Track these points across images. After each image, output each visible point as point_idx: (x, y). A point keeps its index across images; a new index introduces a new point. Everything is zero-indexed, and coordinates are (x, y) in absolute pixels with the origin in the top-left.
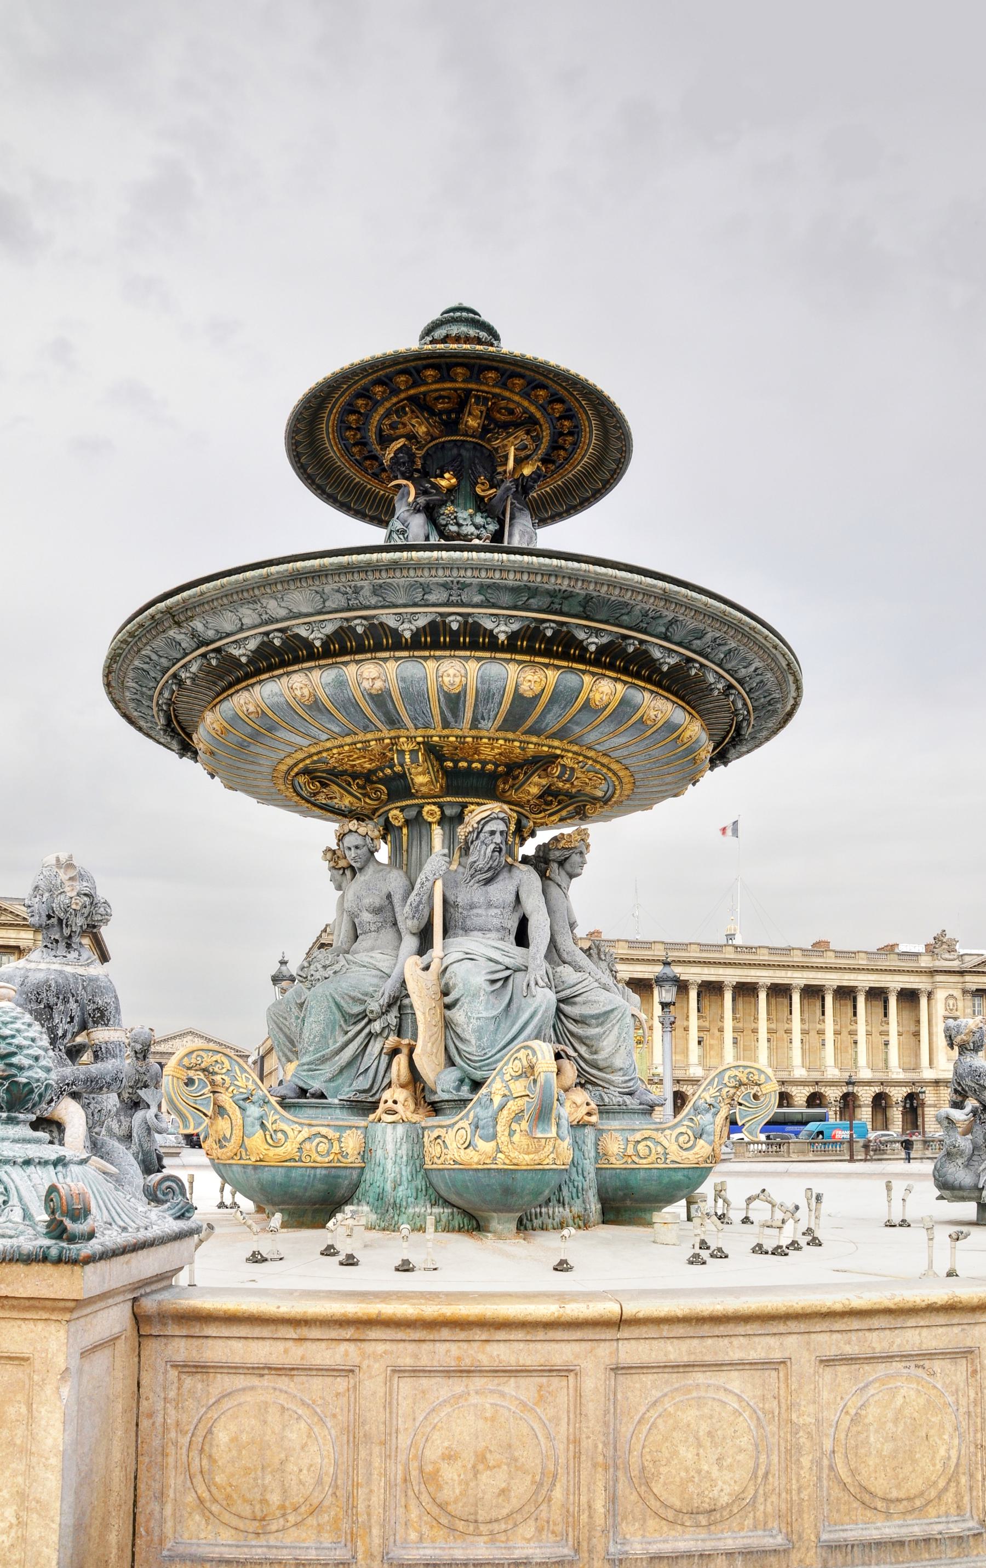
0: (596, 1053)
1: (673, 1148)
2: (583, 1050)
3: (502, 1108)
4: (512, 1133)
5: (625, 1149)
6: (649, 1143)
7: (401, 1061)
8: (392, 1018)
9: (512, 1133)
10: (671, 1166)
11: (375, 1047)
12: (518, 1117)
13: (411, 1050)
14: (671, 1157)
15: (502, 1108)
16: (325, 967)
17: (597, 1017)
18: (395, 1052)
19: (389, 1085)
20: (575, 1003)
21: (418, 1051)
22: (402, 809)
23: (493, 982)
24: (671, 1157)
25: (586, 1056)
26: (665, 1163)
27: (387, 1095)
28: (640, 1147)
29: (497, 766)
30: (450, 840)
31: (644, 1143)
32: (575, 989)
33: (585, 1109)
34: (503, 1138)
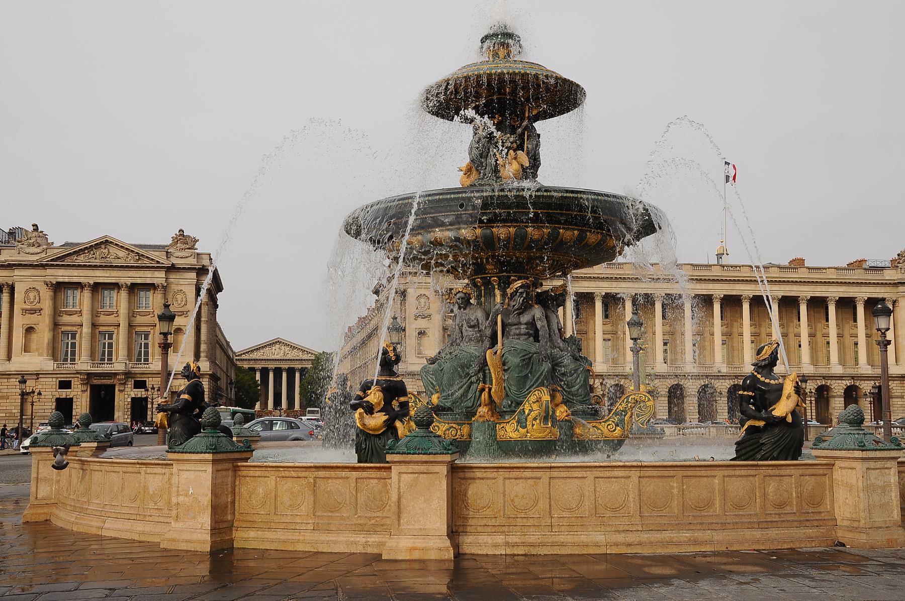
1: (605, 431)
3: (529, 415)
4: (533, 425)
7: (485, 396)
8: (481, 375)
9: (533, 425)
11: (474, 387)
12: (535, 419)
13: (490, 389)
15: (529, 415)
16: (450, 353)
18: (483, 390)
19: (480, 405)
21: (493, 390)
22: (481, 278)
23: (524, 360)
27: (480, 409)
30: (504, 295)
33: (565, 414)
34: (529, 427)
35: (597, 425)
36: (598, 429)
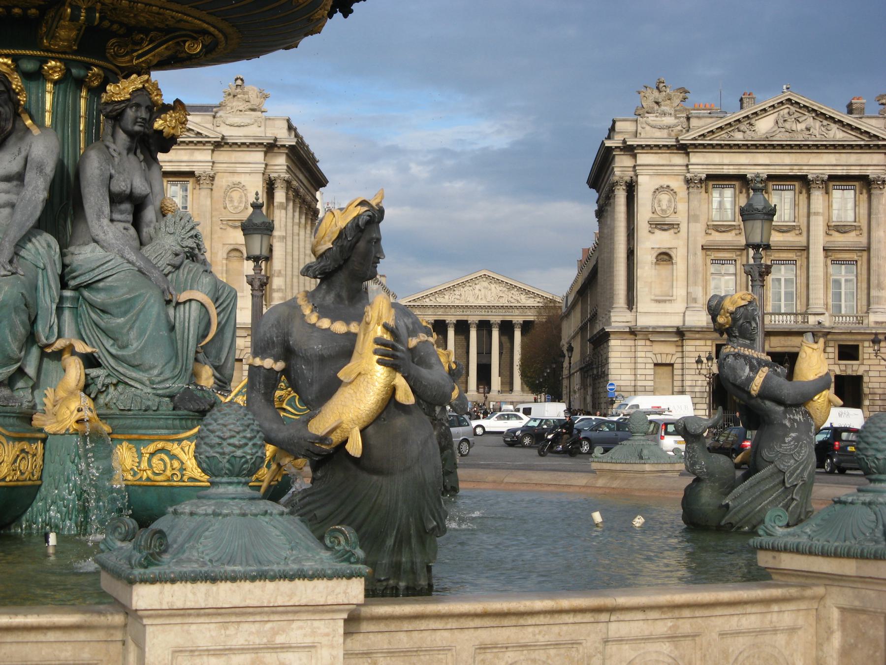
0: (123, 347)
2: (108, 343)
5: (139, 463)
6: (163, 456)
10: (188, 484)
14: (188, 473)
17: (119, 305)
20: (98, 290)
24: (188, 473)
25: (113, 351)
26: (181, 480)
28: (155, 460)
29: (25, 10)
31: (159, 455)
32: (96, 272)
33: (76, 416)
35: (169, 446)
36: (173, 457)
